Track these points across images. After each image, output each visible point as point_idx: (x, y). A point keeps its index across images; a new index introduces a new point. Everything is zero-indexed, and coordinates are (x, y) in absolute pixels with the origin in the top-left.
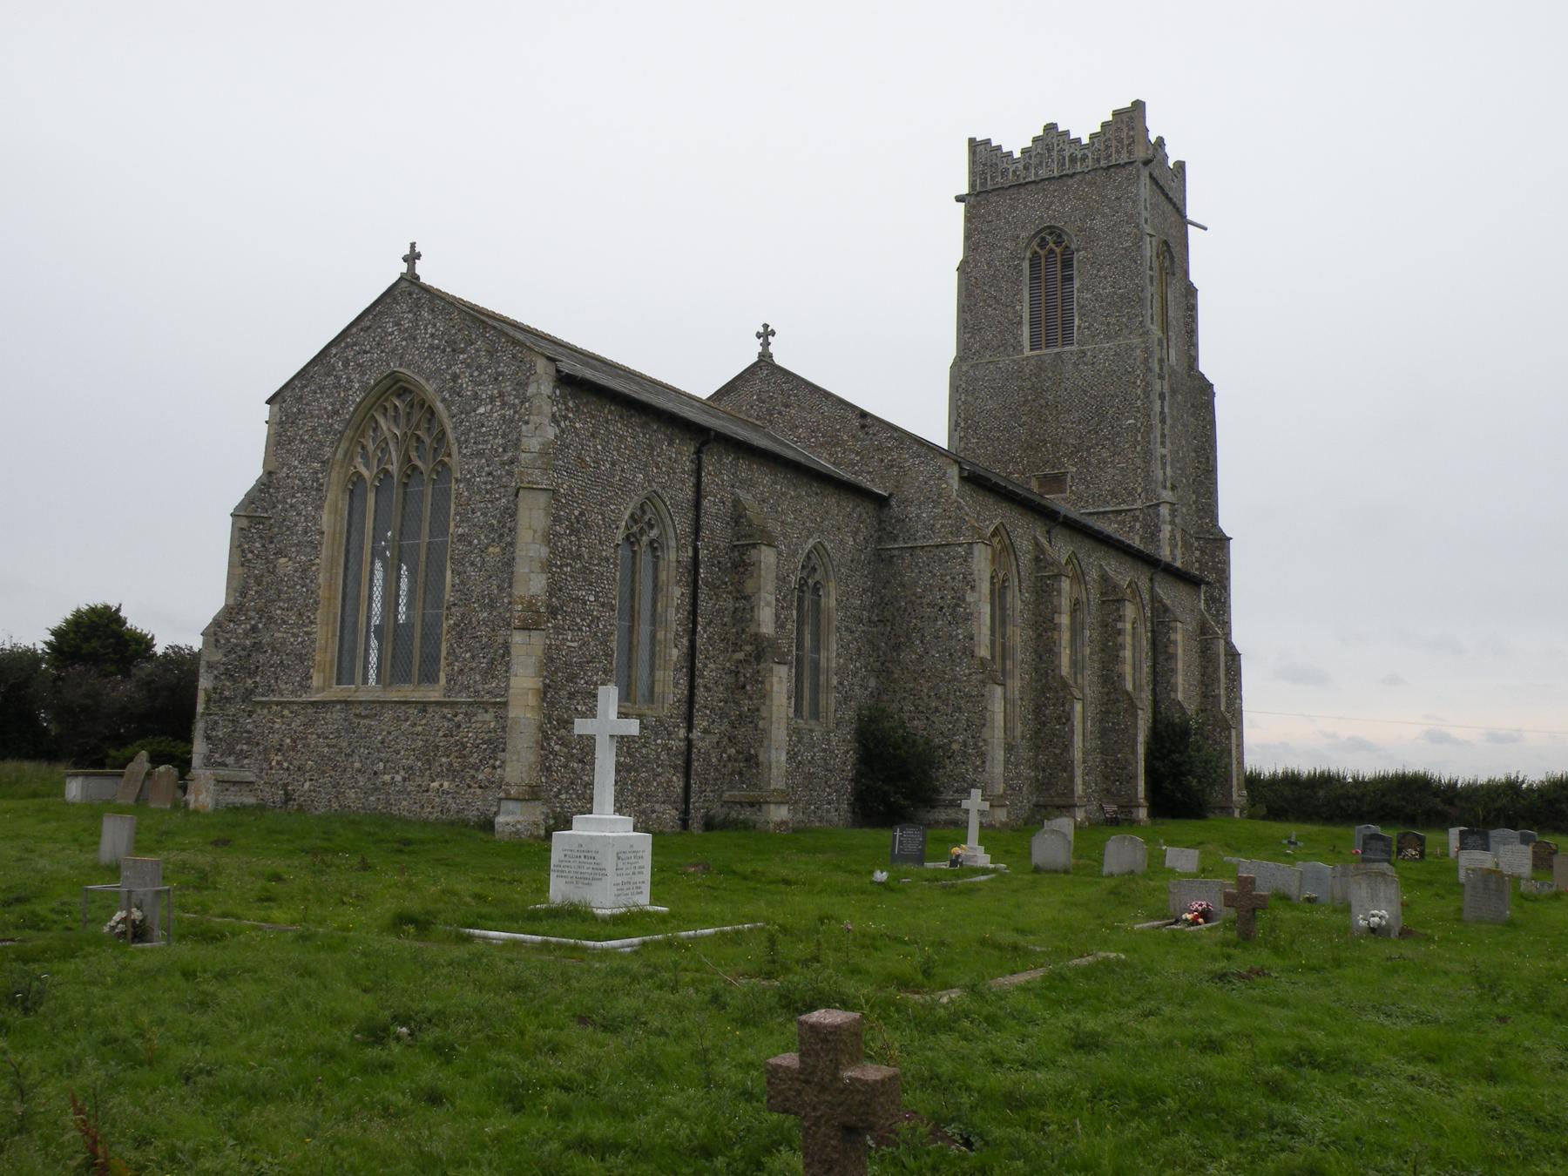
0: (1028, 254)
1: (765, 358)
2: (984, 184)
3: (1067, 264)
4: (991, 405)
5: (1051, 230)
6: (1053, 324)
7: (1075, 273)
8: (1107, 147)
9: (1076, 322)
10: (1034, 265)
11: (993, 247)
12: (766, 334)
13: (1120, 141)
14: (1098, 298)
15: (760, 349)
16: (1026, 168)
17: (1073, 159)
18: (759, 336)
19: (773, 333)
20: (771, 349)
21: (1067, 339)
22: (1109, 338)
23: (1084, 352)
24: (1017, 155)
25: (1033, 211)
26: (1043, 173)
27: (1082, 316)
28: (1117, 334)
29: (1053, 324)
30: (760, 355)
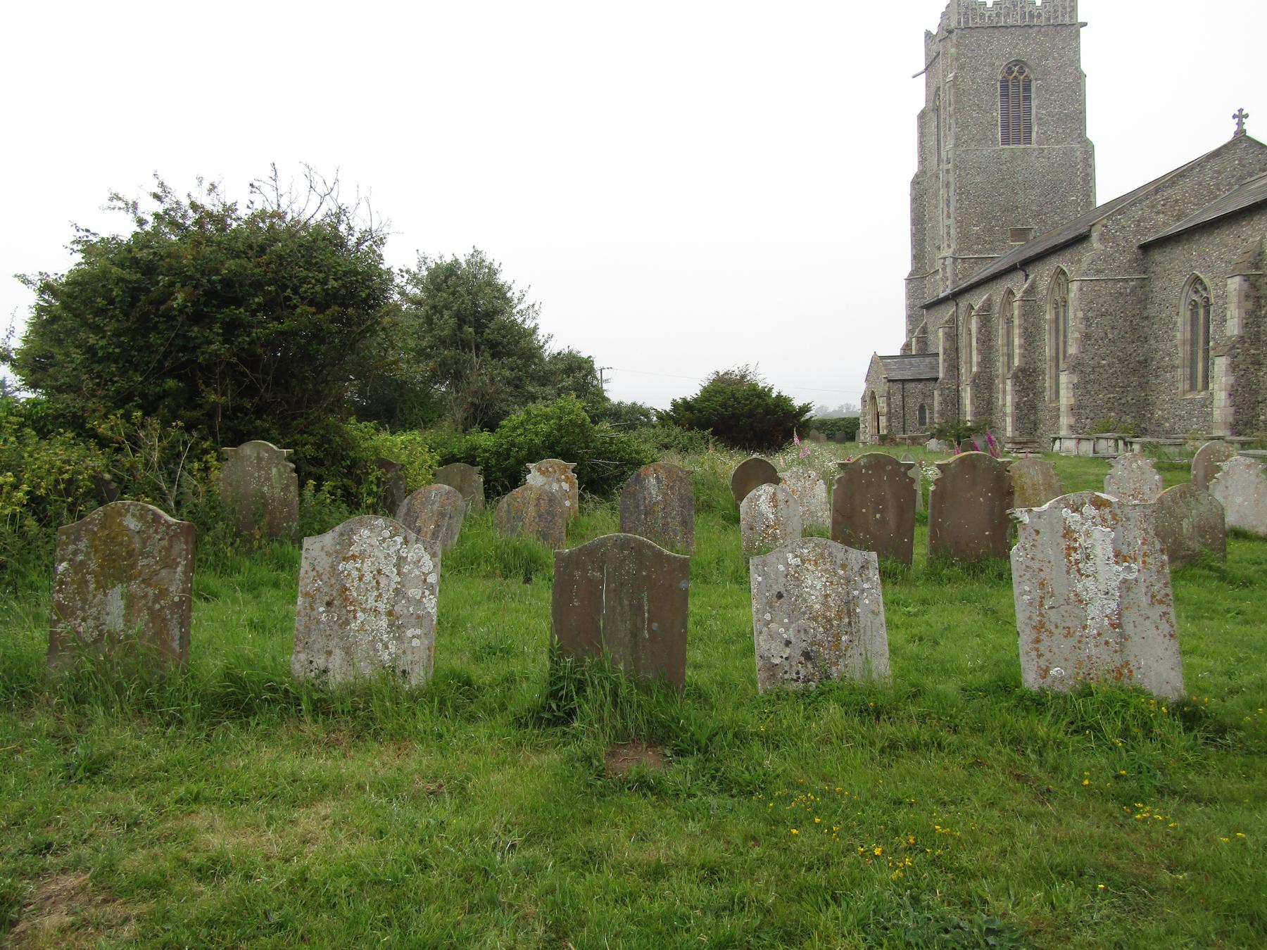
0: (1000, 78)
1: (1240, 136)
2: (967, 22)
3: (1027, 88)
4: (978, 179)
5: (1017, 62)
6: (1016, 129)
7: (1033, 96)
8: (1055, 11)
9: (1035, 129)
10: (1005, 85)
11: (976, 69)
12: (1240, 116)
13: (1065, 8)
14: (1049, 114)
15: (1236, 128)
16: (998, 15)
17: (1031, 16)
18: (1234, 117)
19: (1246, 116)
20: (1245, 127)
21: (1028, 140)
22: (1058, 142)
23: (1043, 150)
24: (990, 5)
25: (1005, 49)
26: (1010, 21)
27: (1039, 125)
28: (1063, 140)
29: (1016, 129)
30: (1236, 133)
